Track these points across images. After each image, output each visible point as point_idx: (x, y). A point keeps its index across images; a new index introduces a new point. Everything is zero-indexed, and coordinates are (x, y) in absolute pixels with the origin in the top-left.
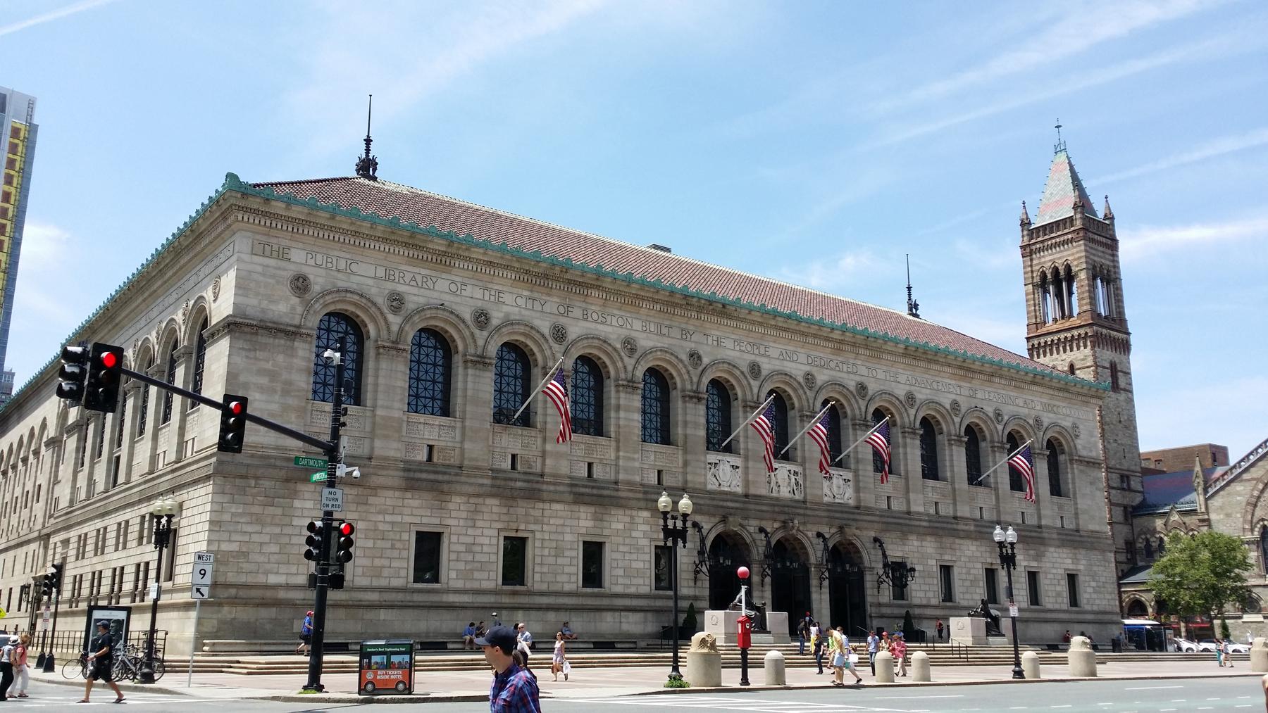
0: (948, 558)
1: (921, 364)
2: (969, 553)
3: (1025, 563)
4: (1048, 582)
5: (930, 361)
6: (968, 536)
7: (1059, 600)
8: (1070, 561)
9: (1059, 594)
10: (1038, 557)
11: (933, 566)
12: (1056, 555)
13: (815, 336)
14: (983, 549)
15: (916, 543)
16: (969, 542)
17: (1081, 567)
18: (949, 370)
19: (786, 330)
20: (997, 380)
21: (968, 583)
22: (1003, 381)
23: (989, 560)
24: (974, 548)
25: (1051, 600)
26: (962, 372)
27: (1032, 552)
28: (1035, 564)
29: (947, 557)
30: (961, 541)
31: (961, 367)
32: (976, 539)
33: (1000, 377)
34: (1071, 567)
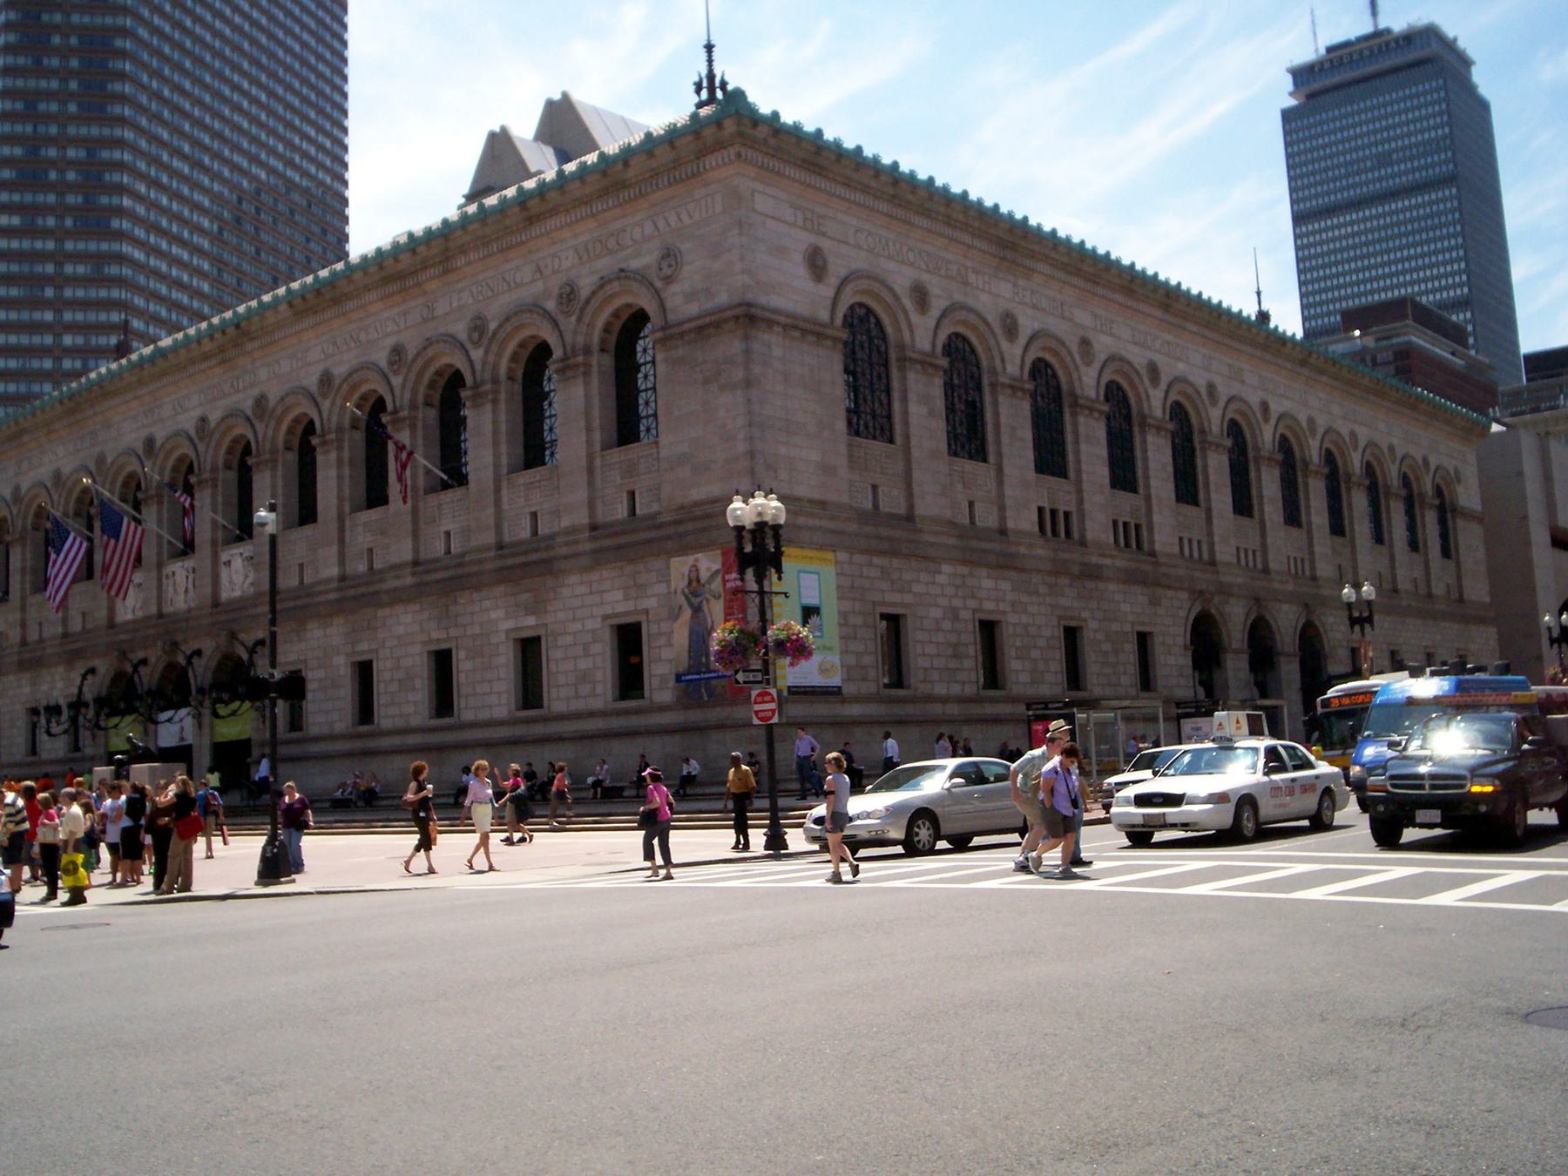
0: (364, 648)
1: (329, 314)
2: (401, 630)
3: (510, 624)
4: (921, 636)
5: (336, 301)
6: (398, 598)
7: (585, 689)
8: (619, 595)
9: (584, 677)
10: (536, 608)
11: (342, 667)
12: (583, 589)
13: (193, 362)
14: (426, 615)
15: (318, 633)
16: (399, 608)
17: (651, 603)
18: (373, 295)
19: (164, 374)
20: (461, 261)
21: (394, 687)
22: (472, 256)
23: (435, 635)
24: (408, 619)
25: (563, 692)
26: (394, 287)
27: (525, 596)
28: (531, 621)
29: (364, 646)
30: (387, 611)
31: (386, 280)
32: (409, 601)
33: (463, 250)
34: (620, 609)
